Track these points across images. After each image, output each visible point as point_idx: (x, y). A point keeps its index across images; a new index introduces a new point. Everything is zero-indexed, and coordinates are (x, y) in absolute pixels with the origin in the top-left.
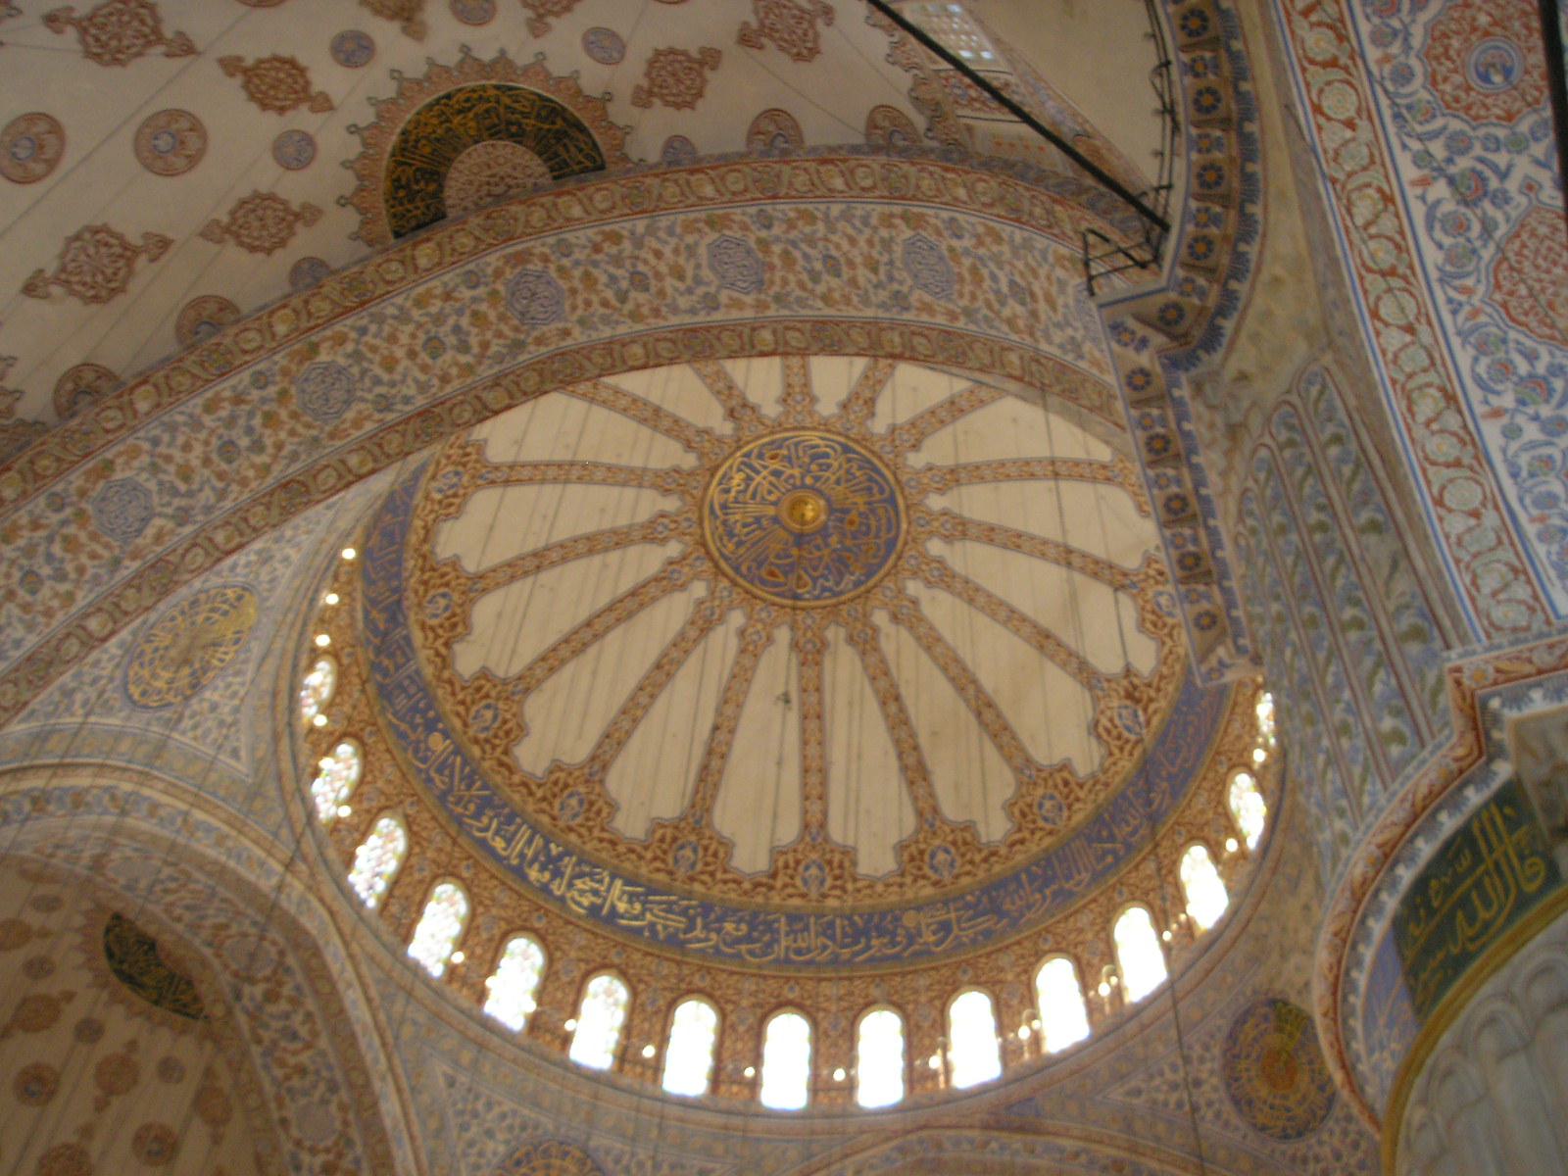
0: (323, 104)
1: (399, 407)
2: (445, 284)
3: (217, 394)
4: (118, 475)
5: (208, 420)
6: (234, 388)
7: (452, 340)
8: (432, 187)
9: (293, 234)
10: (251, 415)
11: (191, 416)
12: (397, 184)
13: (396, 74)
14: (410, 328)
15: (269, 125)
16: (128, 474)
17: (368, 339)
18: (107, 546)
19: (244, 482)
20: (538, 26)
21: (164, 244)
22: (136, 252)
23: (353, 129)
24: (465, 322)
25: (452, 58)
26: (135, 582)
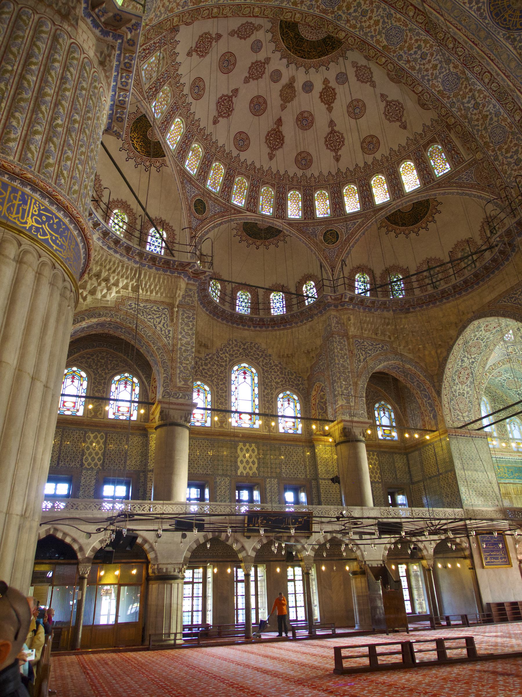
0: (326, 81)
1: (388, 10)
2: (345, 24)
3: (409, 68)
4: (441, 88)
5: (417, 68)
6: (405, 64)
7: (360, 10)
8: (327, 40)
9: (362, 66)
10: (411, 55)
11: (418, 73)
12: (333, 48)
13: (307, 72)
14: (363, 24)
15: (340, 90)
16: (440, 85)
17: (373, 34)
18: (462, 84)
19: (431, 46)
20: (268, 60)
21: (382, 95)
22: (387, 102)
23: (327, 69)
24: (352, 10)
25: (293, 66)
26: (471, 69)
